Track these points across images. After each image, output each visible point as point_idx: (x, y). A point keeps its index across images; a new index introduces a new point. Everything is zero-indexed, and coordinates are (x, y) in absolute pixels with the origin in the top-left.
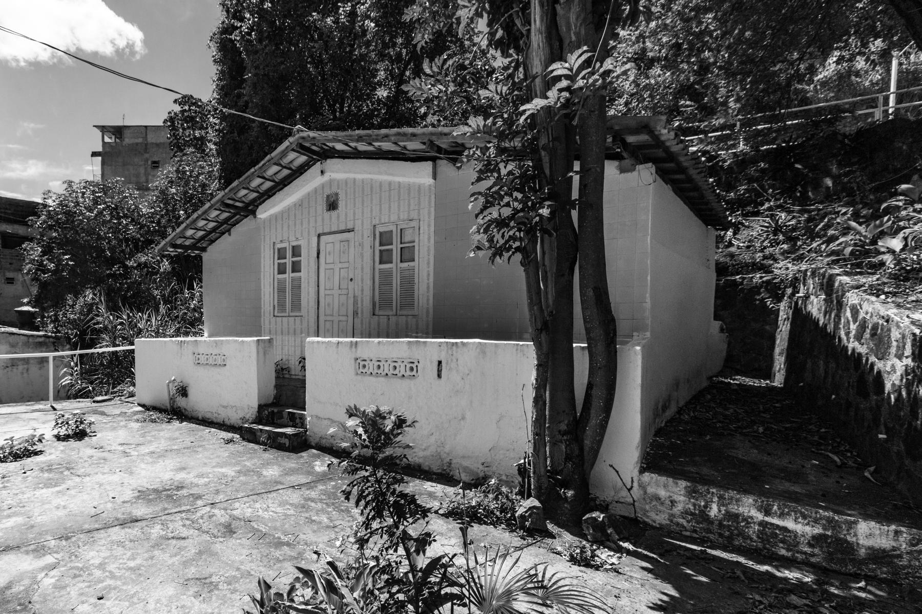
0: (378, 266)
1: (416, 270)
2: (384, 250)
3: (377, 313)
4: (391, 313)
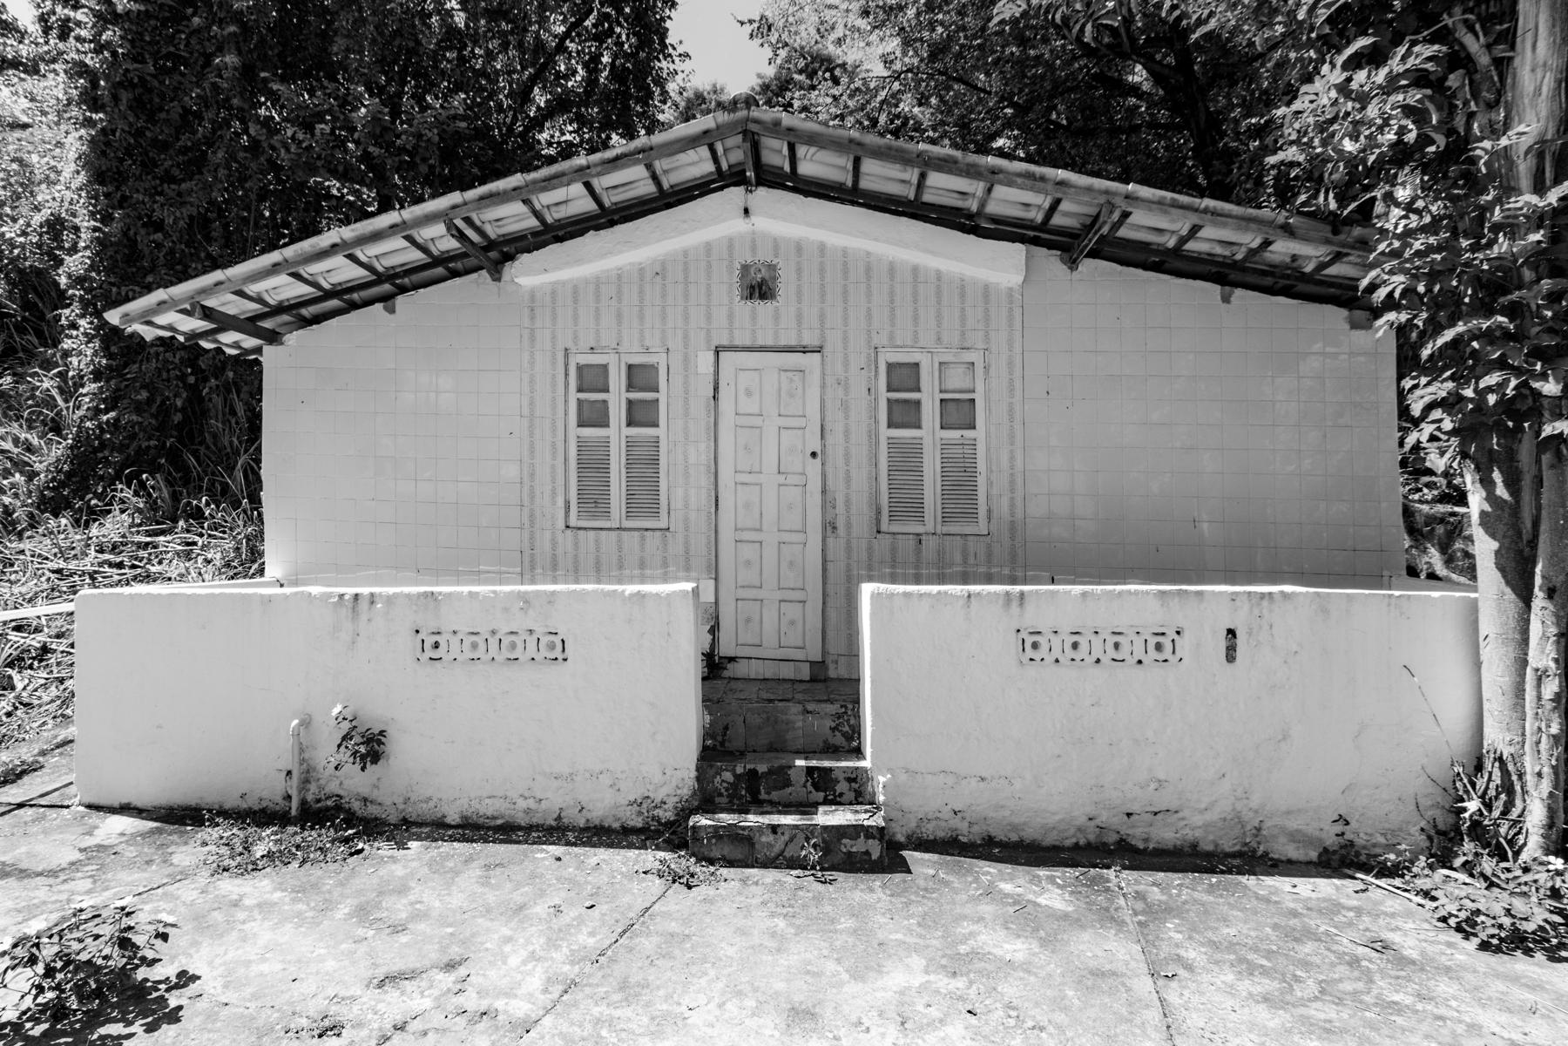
0: (885, 433)
3: (884, 527)
4: (920, 529)
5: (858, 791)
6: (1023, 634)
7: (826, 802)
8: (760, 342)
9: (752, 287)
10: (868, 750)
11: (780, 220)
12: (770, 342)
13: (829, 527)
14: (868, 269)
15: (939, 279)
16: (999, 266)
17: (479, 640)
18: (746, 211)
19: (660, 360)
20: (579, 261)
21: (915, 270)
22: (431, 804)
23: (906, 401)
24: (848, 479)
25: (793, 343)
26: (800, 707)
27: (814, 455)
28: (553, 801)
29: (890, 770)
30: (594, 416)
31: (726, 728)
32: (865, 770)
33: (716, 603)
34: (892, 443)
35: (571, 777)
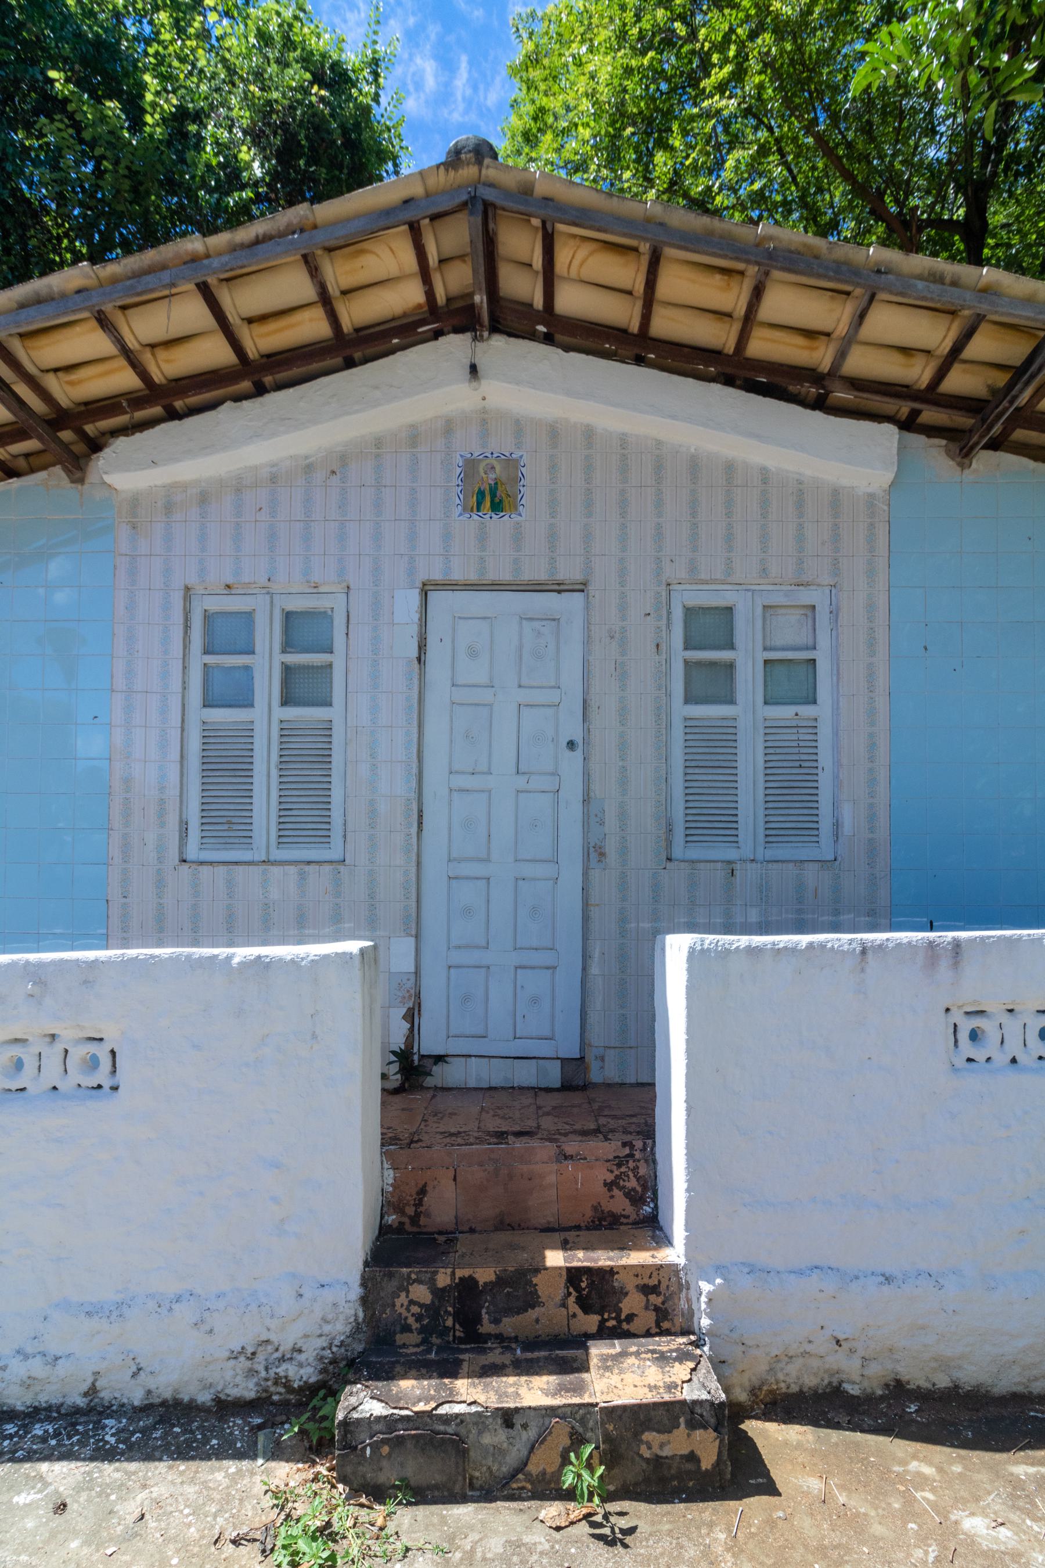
0: (681, 710)
2: (699, 664)
5: (660, 1311)
6: (957, 1017)
7: (605, 1333)
9: (481, 494)
10: (679, 1231)
11: (527, 389)
13: (594, 853)
14: (659, 467)
15: (765, 481)
19: (336, 604)
21: (730, 468)
23: (713, 664)
24: (623, 782)
25: (543, 576)
26: (550, 1149)
27: (571, 745)
29: (720, 1269)
30: (227, 691)
31: (423, 1192)
32: (673, 1269)
33: (417, 973)
34: (691, 725)
35: (118, 1310)
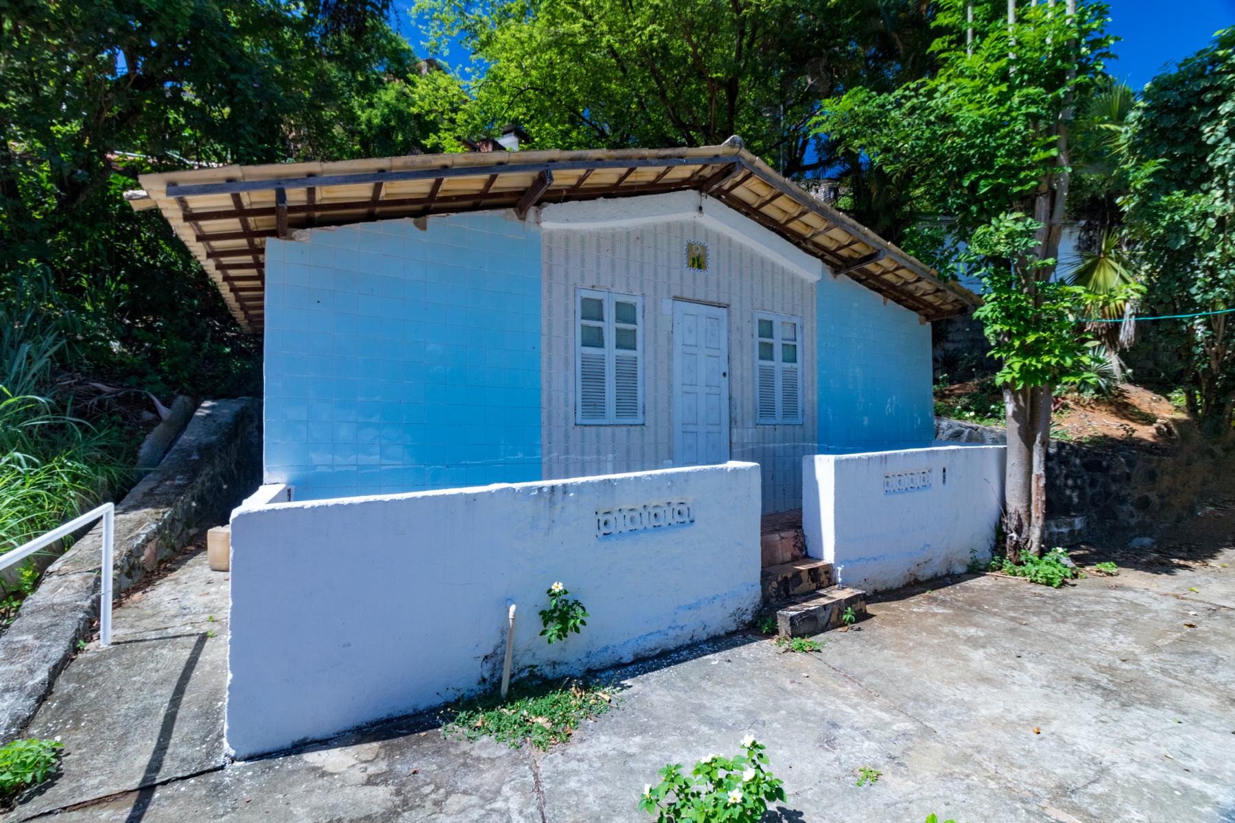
1: (799, 374)
8: (698, 297)
11: (717, 221)
12: (702, 298)
14: (752, 260)
16: (810, 270)
17: (636, 514)
18: (701, 208)
19: (637, 301)
20: (593, 219)
22: (610, 651)
24: (742, 393)
28: (692, 625)
30: (593, 339)
35: (697, 606)
